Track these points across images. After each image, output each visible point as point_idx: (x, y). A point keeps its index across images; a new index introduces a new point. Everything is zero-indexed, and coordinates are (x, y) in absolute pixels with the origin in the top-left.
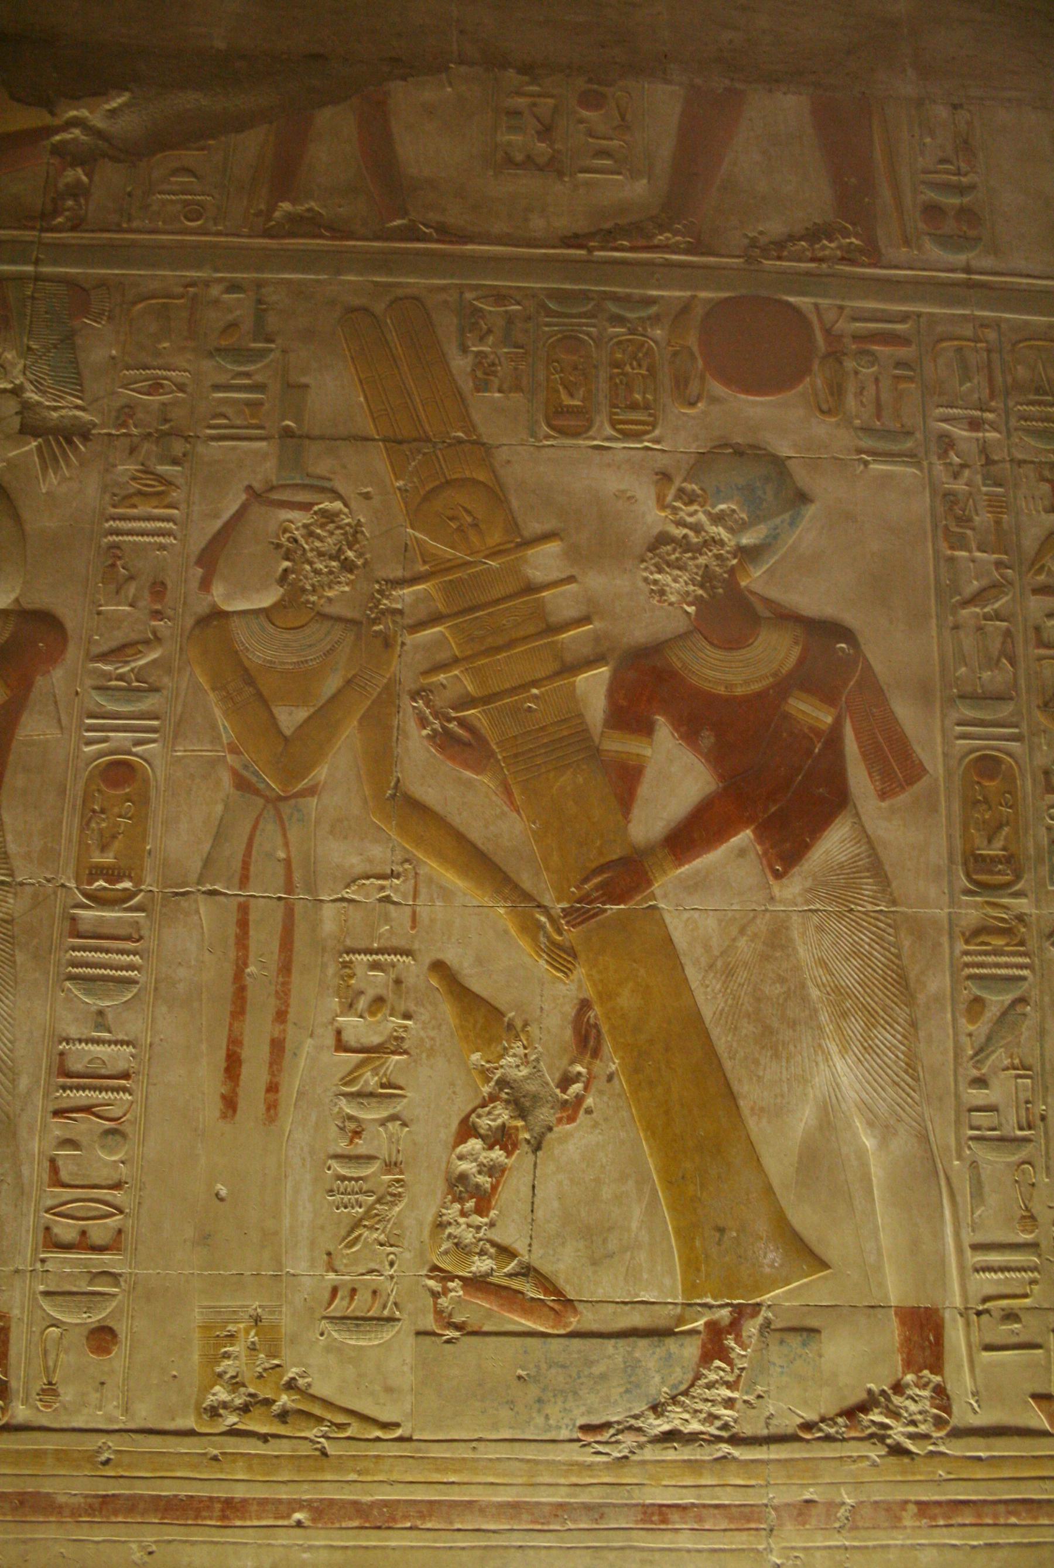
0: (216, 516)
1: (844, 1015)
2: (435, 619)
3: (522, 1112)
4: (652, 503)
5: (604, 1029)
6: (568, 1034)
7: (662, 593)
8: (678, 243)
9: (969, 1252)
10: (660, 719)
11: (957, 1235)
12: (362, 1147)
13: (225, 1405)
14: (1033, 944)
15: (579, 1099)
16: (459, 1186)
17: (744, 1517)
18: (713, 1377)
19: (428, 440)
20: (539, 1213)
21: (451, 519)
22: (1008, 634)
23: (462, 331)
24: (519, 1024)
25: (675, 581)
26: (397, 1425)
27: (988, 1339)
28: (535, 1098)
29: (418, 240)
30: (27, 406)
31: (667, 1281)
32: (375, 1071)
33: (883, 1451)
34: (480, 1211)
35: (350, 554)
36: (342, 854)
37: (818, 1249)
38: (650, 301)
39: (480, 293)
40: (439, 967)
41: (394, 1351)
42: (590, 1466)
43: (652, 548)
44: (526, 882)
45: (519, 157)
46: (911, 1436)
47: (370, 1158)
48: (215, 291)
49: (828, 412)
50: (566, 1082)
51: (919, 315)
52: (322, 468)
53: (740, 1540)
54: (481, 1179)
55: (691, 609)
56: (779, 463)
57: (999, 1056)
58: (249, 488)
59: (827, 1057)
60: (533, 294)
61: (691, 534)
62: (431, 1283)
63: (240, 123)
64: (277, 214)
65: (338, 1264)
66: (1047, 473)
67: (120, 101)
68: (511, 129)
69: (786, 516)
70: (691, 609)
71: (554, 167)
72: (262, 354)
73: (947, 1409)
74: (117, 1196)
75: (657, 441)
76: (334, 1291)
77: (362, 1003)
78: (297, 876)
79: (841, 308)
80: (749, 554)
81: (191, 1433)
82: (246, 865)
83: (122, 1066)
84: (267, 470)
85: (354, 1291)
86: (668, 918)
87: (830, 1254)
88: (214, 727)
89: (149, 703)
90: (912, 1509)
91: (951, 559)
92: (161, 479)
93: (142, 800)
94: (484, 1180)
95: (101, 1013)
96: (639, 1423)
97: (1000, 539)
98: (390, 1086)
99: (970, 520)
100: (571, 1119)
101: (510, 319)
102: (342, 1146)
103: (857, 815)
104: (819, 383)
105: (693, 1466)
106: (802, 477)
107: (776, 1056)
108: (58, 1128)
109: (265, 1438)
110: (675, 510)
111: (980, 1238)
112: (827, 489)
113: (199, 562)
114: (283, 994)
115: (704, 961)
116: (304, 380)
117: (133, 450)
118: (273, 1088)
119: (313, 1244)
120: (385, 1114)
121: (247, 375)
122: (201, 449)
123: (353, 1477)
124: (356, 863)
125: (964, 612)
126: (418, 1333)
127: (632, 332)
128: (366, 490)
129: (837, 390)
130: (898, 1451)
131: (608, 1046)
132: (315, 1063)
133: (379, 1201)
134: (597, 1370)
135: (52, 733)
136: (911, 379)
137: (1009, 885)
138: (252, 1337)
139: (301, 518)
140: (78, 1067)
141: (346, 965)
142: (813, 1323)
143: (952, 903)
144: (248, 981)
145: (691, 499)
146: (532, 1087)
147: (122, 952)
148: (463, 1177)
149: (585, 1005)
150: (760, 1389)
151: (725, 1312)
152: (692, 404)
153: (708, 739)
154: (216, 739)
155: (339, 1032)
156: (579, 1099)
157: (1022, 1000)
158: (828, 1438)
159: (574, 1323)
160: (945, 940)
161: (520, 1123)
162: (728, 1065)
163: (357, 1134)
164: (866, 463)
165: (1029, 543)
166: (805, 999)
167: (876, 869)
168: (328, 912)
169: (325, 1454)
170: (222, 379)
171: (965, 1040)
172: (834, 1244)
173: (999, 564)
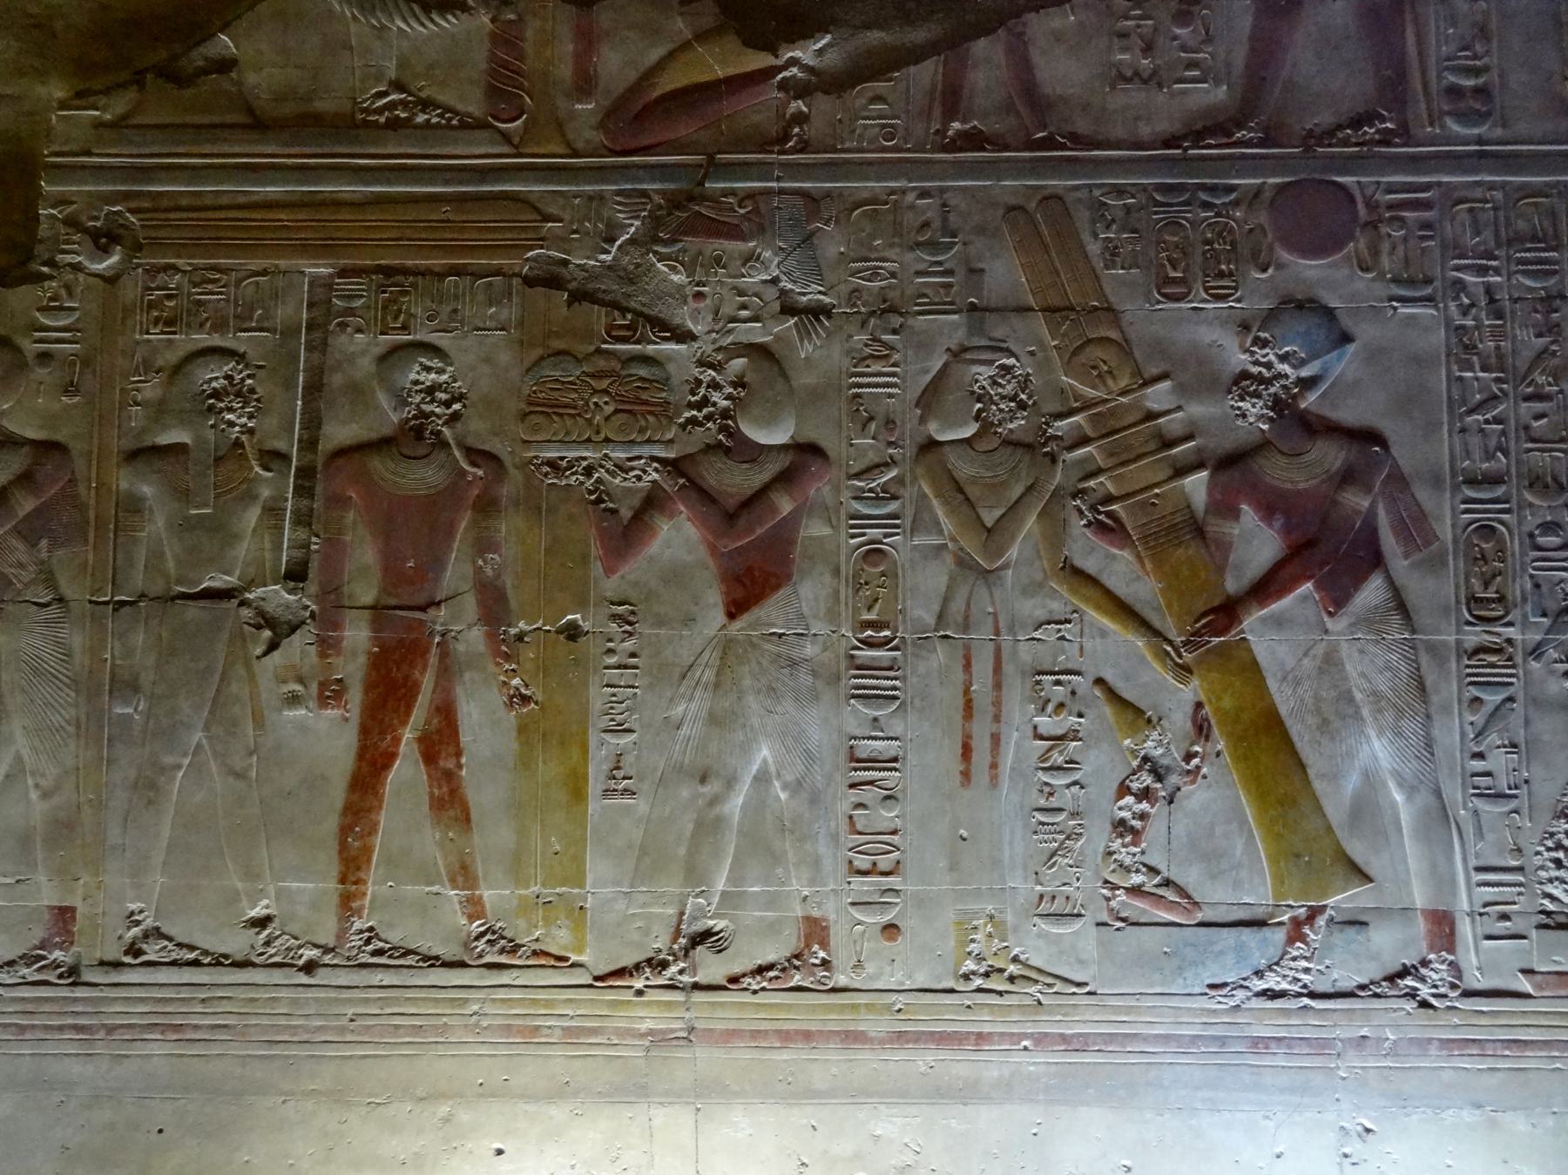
0: (927, 372)
1: (1380, 711)
2: (1084, 441)
3: (1159, 778)
4: (1236, 349)
5: (1213, 722)
6: (1189, 724)
7: (1244, 416)
8: (1252, 139)
9: (1473, 873)
10: (1244, 507)
11: (1465, 860)
12: (1054, 802)
13: (973, 973)
14: (1519, 659)
15: (1198, 768)
16: (1121, 827)
17: (1321, 1046)
18: (1295, 953)
19: (1073, 309)
20: (1174, 845)
21: (1094, 367)
22: (1503, 433)
23: (1093, 222)
24: (1155, 719)
25: (1254, 406)
26: (1086, 984)
27: (1488, 931)
28: (1168, 769)
29: (1056, 149)
30: (783, 292)
31: (1262, 890)
32: (1061, 752)
33: (1415, 1005)
34: (1134, 844)
35: (1023, 397)
36: (1034, 608)
37: (1366, 869)
38: (1231, 189)
39: (1105, 190)
40: (1100, 681)
41: (1080, 934)
42: (1215, 1011)
43: (1236, 383)
44: (1157, 624)
45: (1129, 74)
46: (1434, 995)
47: (1060, 810)
48: (910, 197)
49: (1367, 270)
50: (1189, 757)
51: (1439, 184)
52: (998, 334)
53: (1317, 1062)
54: (1134, 823)
55: (1265, 427)
56: (1329, 313)
57: (1493, 738)
58: (948, 349)
59: (1368, 738)
60: (1144, 188)
61: (1264, 371)
62: (1105, 891)
63: (916, 55)
64: (950, 133)
65: (1042, 879)
66: (1539, 307)
67: (824, 42)
68: (1124, 50)
69: (1335, 353)
70: (1265, 427)
71: (1152, 79)
72: (951, 245)
73: (1460, 978)
74: (895, 839)
75: (1238, 300)
76: (1042, 897)
77: (1050, 708)
78: (1002, 624)
79: (1378, 183)
80: (1308, 384)
81: (952, 991)
82: (967, 617)
83: (893, 753)
84: (959, 337)
85: (1054, 897)
86: (1253, 647)
87: (1371, 873)
88: (939, 523)
89: (893, 507)
90: (1436, 1043)
91: (1460, 379)
92: (884, 344)
93: (891, 574)
94: (1137, 824)
95: (875, 719)
96: (1246, 983)
97: (1498, 362)
98: (1071, 762)
99: (1475, 347)
100: (1193, 782)
101: (1128, 209)
102: (1042, 802)
103: (1387, 571)
104: (1362, 244)
105: (1285, 1012)
106: (1346, 322)
107: (1333, 739)
108: (854, 795)
109: (1000, 993)
110: (1253, 353)
111: (1481, 863)
112: (1366, 332)
113: (917, 405)
114: (997, 704)
115: (1279, 676)
116: (981, 265)
117: (864, 324)
118: (994, 766)
119: (1025, 867)
120: (1068, 781)
121: (940, 263)
122: (910, 322)
123: (1059, 1018)
124: (1041, 614)
125: (1469, 419)
126: (1098, 924)
127: (1218, 215)
128: (1032, 347)
129: (1375, 252)
130: (1424, 1004)
131: (1216, 731)
132: (1019, 748)
133: (1068, 838)
134: (1217, 948)
135: (826, 531)
136: (1431, 238)
137: (1501, 617)
138: (989, 928)
139: (985, 372)
140: (864, 756)
141: (1038, 683)
142: (1363, 918)
143: (1458, 632)
144: (974, 696)
145: (1264, 344)
146: (1165, 761)
147: (887, 678)
148: (1122, 822)
149: (1199, 705)
150: (1328, 962)
151: (1302, 910)
152: (1264, 270)
153: (1279, 522)
154: (941, 532)
155: (1035, 727)
156: (1198, 768)
157: (1511, 699)
158: (1376, 995)
159: (1199, 916)
160: (1453, 658)
161: (1159, 785)
162: (1298, 745)
163: (1051, 794)
164: (1395, 309)
165: (1522, 366)
166: (1351, 700)
167: (1401, 606)
168: (1023, 647)
169: (1040, 1003)
170: (921, 267)
171: (1469, 729)
172: (1373, 866)
173: (1498, 380)
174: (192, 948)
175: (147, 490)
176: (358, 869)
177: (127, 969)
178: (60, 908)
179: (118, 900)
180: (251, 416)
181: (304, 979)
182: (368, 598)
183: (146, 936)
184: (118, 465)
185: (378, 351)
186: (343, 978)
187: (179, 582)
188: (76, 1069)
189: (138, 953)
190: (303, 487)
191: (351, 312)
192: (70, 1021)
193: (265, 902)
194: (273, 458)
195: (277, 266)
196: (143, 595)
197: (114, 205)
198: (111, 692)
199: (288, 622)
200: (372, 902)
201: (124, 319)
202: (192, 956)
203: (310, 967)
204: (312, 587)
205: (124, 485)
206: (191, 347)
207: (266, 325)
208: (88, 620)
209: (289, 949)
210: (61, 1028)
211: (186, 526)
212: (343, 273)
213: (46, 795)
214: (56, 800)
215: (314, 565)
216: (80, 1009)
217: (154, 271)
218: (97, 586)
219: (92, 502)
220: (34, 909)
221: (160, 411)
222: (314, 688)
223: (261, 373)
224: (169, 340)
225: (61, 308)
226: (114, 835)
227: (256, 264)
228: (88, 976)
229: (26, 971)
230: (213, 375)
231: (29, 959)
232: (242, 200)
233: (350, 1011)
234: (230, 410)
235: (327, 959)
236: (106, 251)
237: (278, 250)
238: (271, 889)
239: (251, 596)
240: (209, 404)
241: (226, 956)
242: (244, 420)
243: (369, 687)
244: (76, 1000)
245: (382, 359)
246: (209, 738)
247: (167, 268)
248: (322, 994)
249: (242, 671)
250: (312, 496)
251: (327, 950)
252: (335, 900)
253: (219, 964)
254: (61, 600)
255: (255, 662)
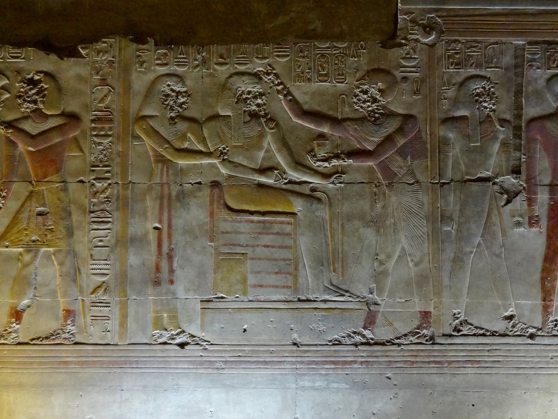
174: (482, 329)
175: (451, 135)
176: (551, 295)
177: (455, 338)
178: (425, 312)
179: (451, 307)
180: (494, 105)
181: (530, 341)
182: (547, 181)
183: (461, 324)
184: (439, 125)
185: (547, 77)
186: (547, 341)
187: (467, 174)
188: (437, 379)
189: (459, 331)
190: (516, 135)
191: (534, 60)
192: (432, 359)
193: (512, 309)
194: (503, 122)
195: (501, 40)
196: (452, 180)
197: (431, 14)
198: (441, 221)
199: (514, 192)
200: (556, 309)
201: (438, 62)
202: (481, 332)
203: (532, 336)
204: (524, 176)
205: (442, 133)
206: (466, 75)
207: (498, 65)
208: (430, 190)
209: (522, 329)
210: (429, 362)
211: (470, 151)
212: (530, 43)
213: (416, 265)
214: (422, 266)
215: (523, 168)
216: (436, 354)
217: (448, 43)
218: (433, 176)
219: (429, 141)
220: (414, 313)
221: (456, 103)
222: (527, 219)
223: (497, 86)
224: (459, 72)
225: (411, 58)
226: (446, 281)
227: (493, 40)
228: (438, 340)
229: (412, 338)
230: (477, 86)
231: (413, 334)
232: (485, 12)
233: (550, 355)
234: (485, 101)
235: (539, 333)
236: (429, 34)
237: (502, 34)
238: (513, 304)
239: (497, 180)
240: (476, 99)
241: (496, 332)
242: (491, 106)
243: (550, 218)
244: (434, 350)
245: (549, 80)
246: (483, 240)
247: (455, 41)
248: (538, 348)
249: (496, 212)
250: (521, 139)
251: (539, 329)
252: (541, 308)
253: (493, 335)
254: (417, 182)
255: (501, 209)
